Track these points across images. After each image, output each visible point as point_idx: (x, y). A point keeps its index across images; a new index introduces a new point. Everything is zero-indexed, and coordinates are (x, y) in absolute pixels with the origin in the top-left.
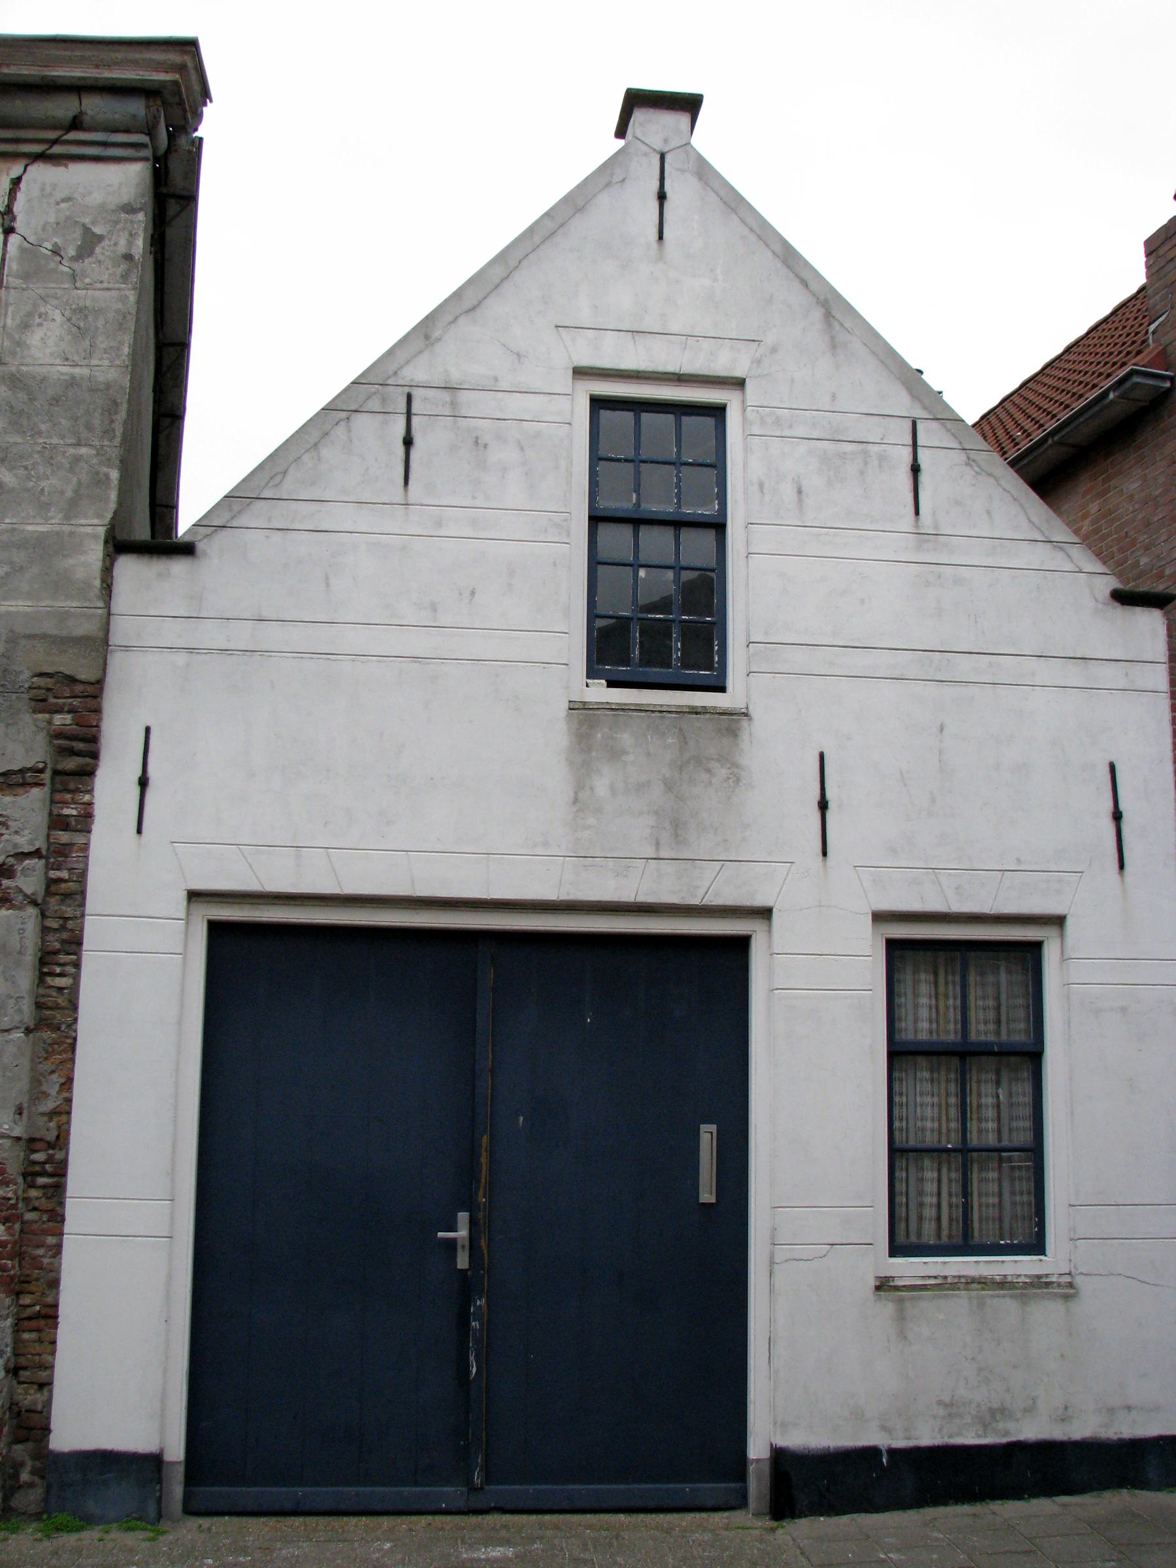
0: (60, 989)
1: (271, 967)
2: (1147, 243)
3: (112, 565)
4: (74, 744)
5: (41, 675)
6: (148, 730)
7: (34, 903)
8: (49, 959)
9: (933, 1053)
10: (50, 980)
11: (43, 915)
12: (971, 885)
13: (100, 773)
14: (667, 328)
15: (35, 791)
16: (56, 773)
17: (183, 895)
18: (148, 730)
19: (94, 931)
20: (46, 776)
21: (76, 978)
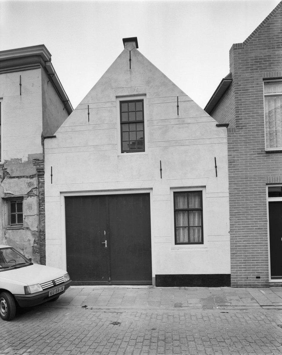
0: (42, 208)
1: (74, 203)
2: (234, 45)
3: (44, 141)
4: (40, 170)
5: (34, 160)
6: (52, 167)
7: (36, 195)
8: (40, 204)
9: (183, 210)
10: (41, 207)
11: (39, 197)
12: (189, 182)
13: (45, 174)
14: (132, 85)
15: (34, 178)
16: (38, 175)
17: (59, 193)
18: (52, 167)
19: (46, 199)
20: (37, 175)
21: (44, 207)
